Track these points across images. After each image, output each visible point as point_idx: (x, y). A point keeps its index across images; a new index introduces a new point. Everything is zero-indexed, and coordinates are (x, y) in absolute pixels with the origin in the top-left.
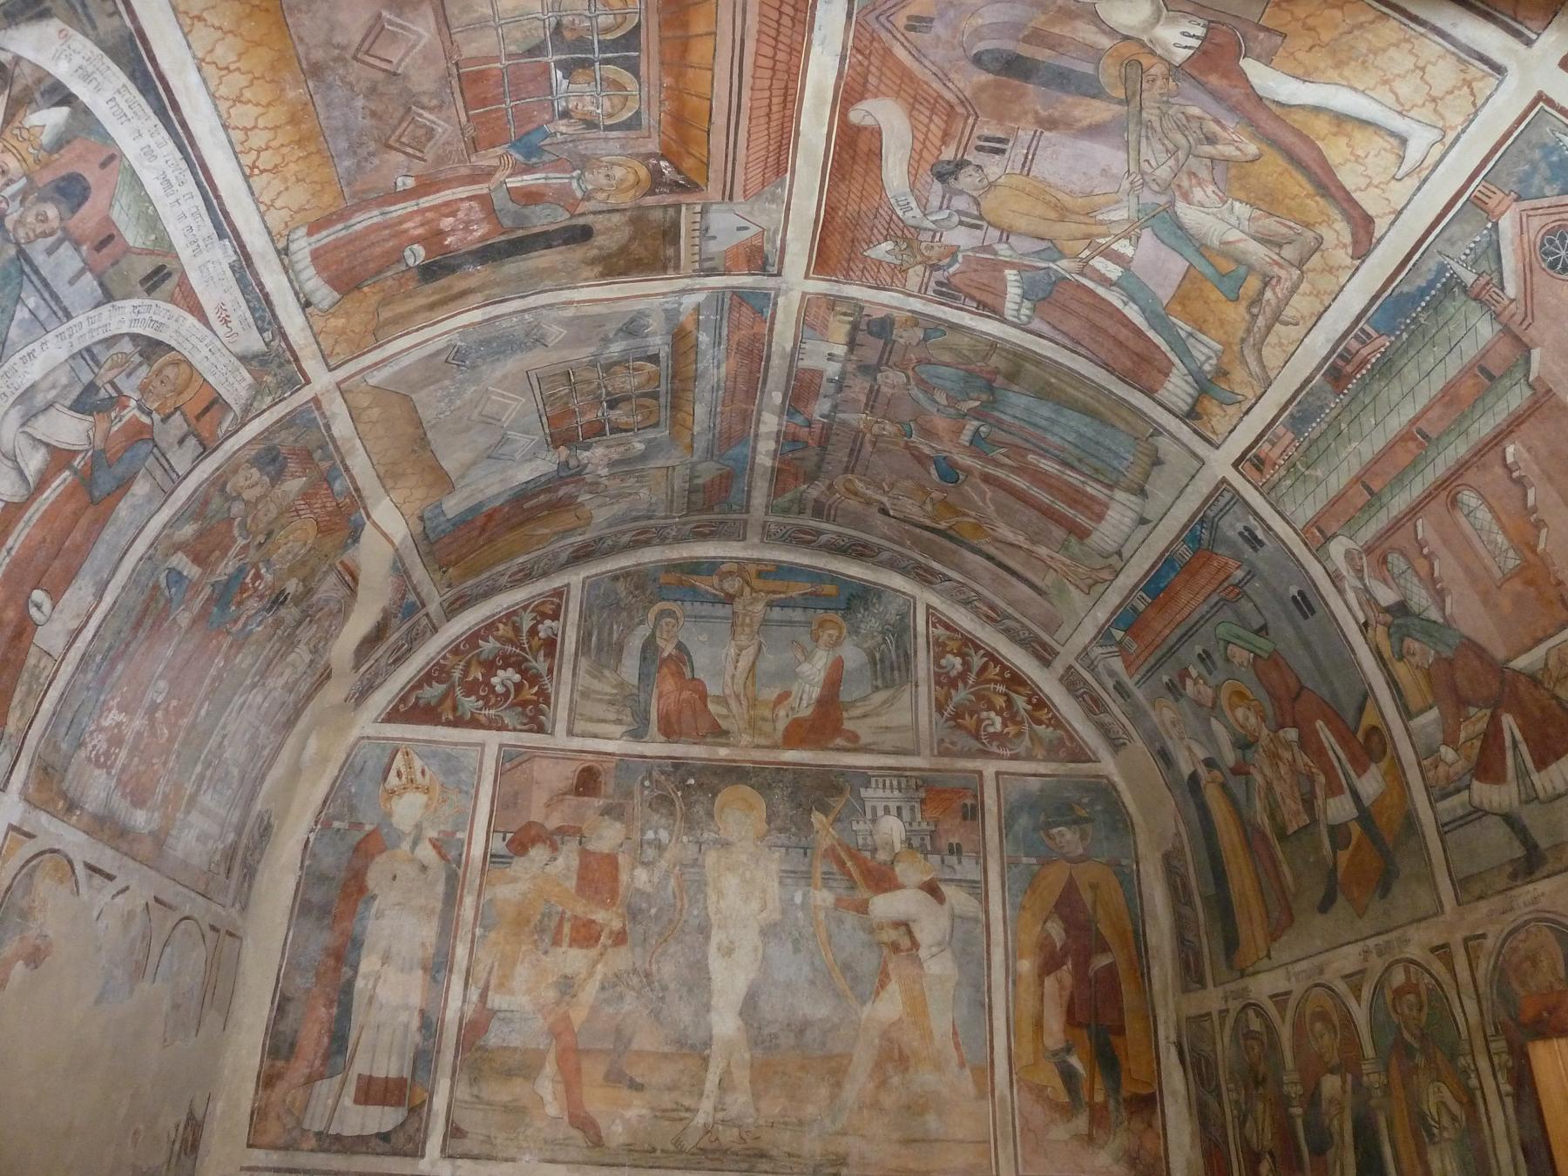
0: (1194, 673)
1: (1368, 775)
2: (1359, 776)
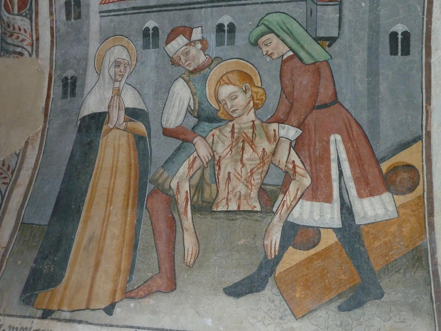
0: (197, 34)
1: (375, 199)
2: (360, 196)
